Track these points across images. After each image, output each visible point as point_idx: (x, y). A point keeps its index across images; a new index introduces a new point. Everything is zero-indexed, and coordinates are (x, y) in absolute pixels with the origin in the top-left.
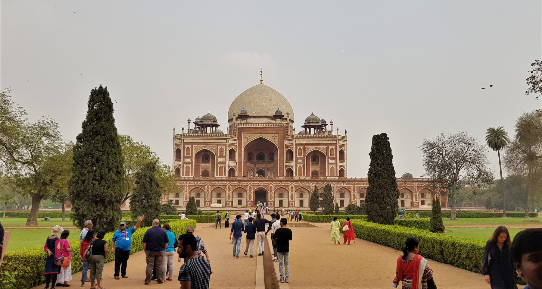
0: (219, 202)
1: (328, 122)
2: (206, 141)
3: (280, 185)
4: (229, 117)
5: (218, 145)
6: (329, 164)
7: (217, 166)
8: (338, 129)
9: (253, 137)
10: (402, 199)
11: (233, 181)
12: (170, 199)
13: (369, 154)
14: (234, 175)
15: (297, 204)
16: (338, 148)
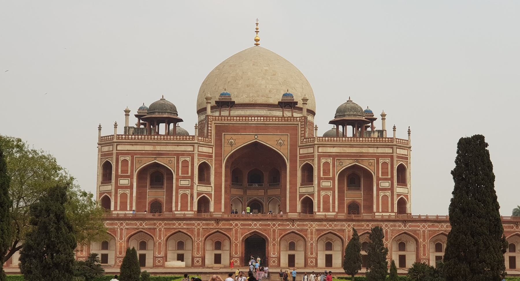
0: (180, 258)
1: (377, 115)
2: (158, 148)
3: (290, 227)
4: (199, 105)
5: (178, 155)
6: (378, 190)
7: (177, 193)
8: (394, 128)
9: (242, 140)
10: (512, 254)
12: (92, 252)
13: (452, 173)
14: (207, 210)
15: (321, 262)
16: (395, 162)
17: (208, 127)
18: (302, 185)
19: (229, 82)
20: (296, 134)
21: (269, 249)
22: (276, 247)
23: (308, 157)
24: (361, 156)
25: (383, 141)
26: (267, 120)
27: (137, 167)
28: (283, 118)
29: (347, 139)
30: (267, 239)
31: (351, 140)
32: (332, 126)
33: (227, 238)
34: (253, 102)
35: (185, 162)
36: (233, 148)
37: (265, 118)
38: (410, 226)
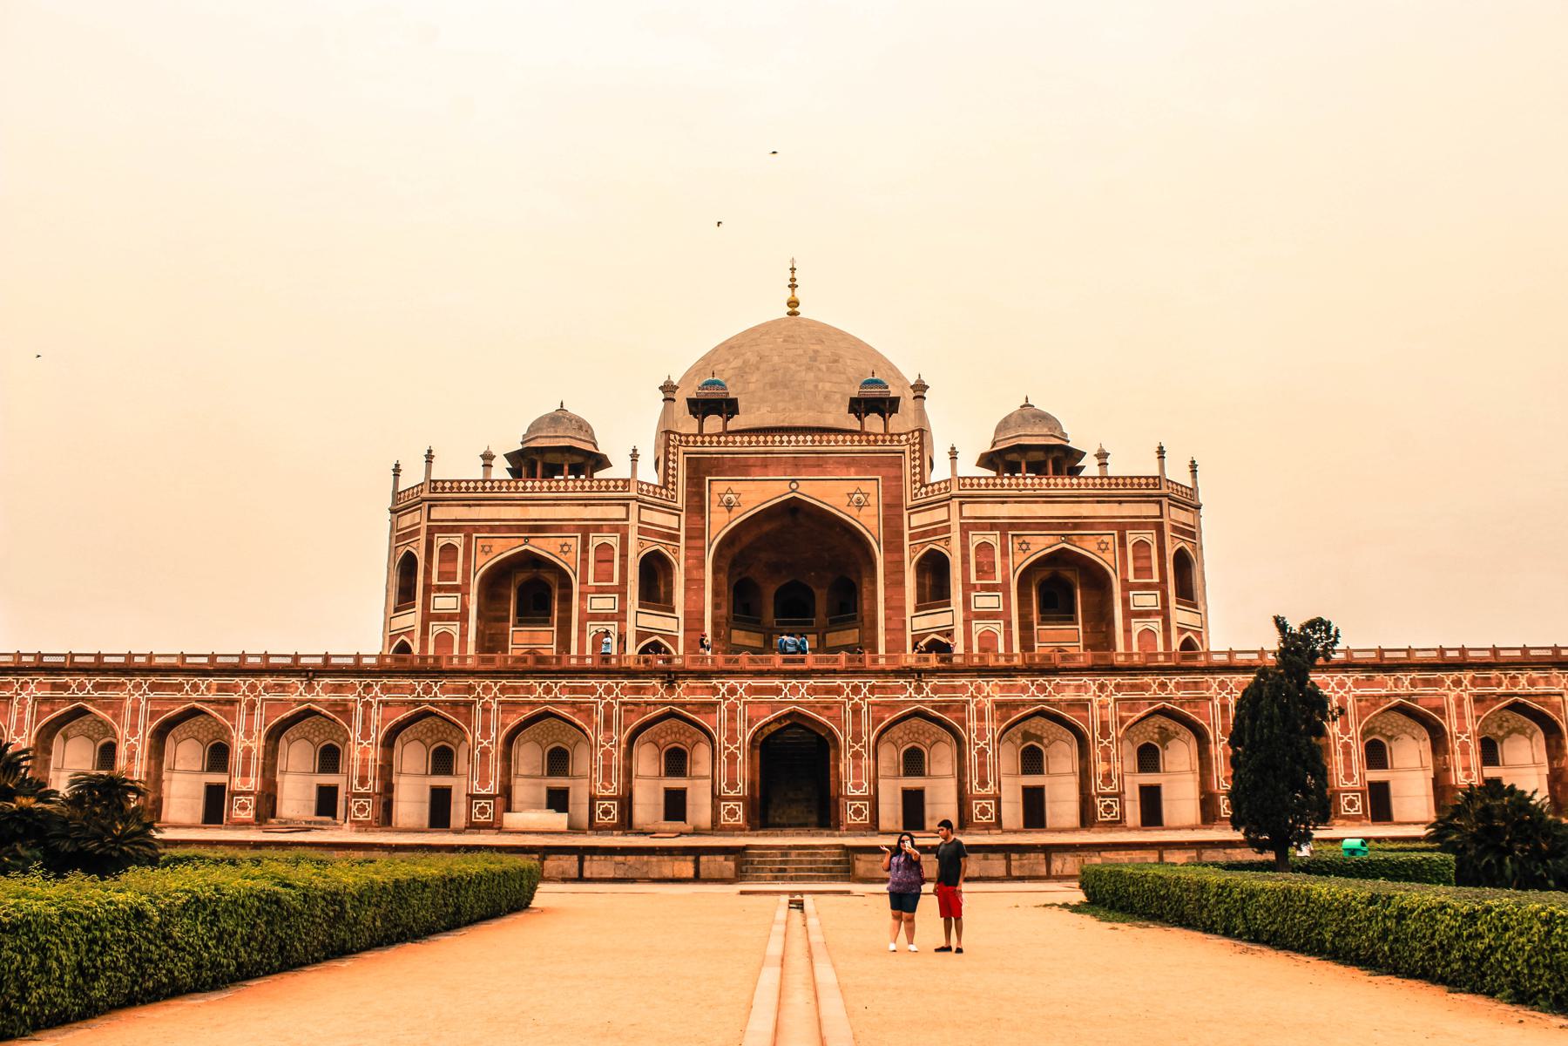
0: (558, 801)
3: (908, 695)
5: (586, 531)
6: (1129, 615)
7: (582, 631)
11: (630, 673)
16: (1168, 540)
17: (667, 460)
18: (917, 609)
21: (842, 769)
22: (866, 762)
27: (479, 564)
30: (835, 739)
31: (1048, 485)
34: (786, 424)
35: (605, 548)
36: (733, 515)
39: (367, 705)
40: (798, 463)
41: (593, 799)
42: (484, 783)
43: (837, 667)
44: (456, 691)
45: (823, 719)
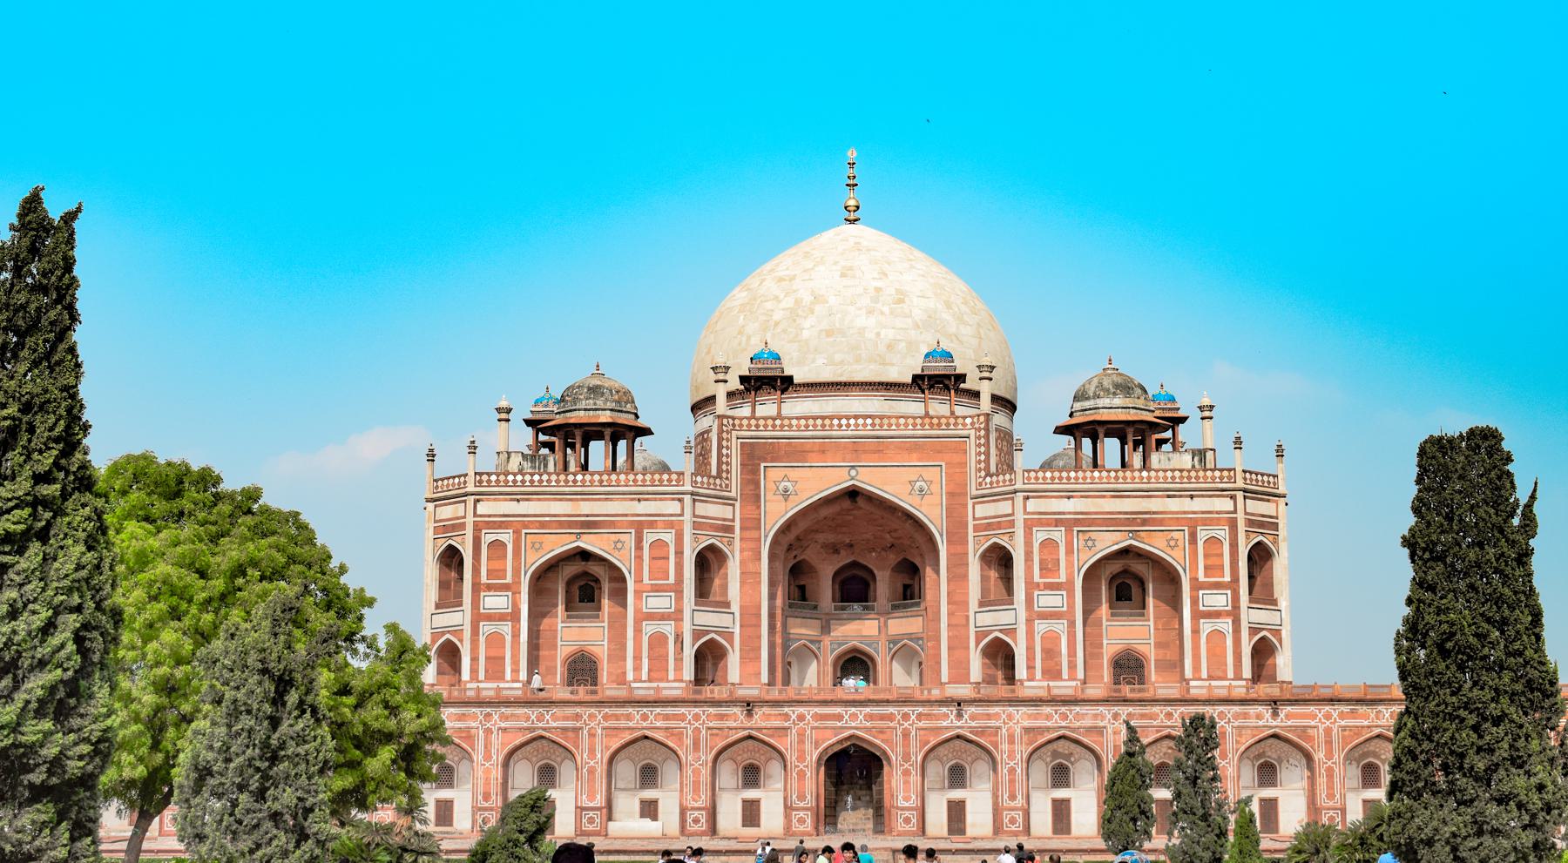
0: (649, 810)
2: (586, 508)
5: (639, 527)
6: (1198, 615)
7: (638, 631)
8: (1238, 443)
17: (720, 447)
18: (981, 604)
19: (777, 324)
20: (963, 464)
23: (999, 526)
24: (1144, 522)
25: (1205, 477)
26: (881, 425)
28: (927, 421)
29: (1104, 474)
31: (1117, 478)
32: (1066, 441)
33: (776, 755)
34: (843, 379)
35: (659, 544)
36: (790, 505)
37: (877, 421)
38: (1288, 716)
39: (488, 732)
40: (858, 449)
41: (683, 812)
42: (591, 797)
43: (890, 698)
44: (566, 718)
45: (877, 742)
